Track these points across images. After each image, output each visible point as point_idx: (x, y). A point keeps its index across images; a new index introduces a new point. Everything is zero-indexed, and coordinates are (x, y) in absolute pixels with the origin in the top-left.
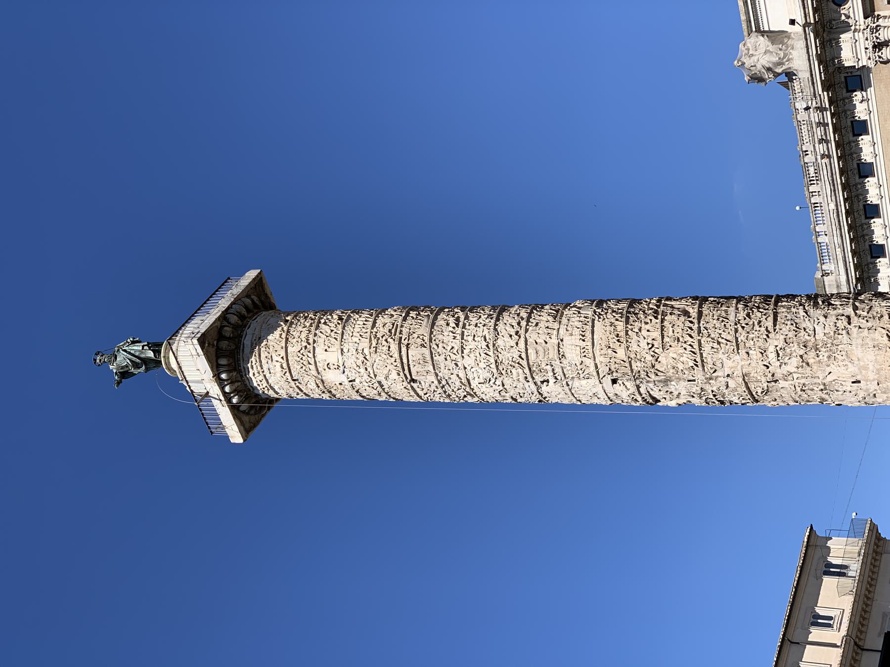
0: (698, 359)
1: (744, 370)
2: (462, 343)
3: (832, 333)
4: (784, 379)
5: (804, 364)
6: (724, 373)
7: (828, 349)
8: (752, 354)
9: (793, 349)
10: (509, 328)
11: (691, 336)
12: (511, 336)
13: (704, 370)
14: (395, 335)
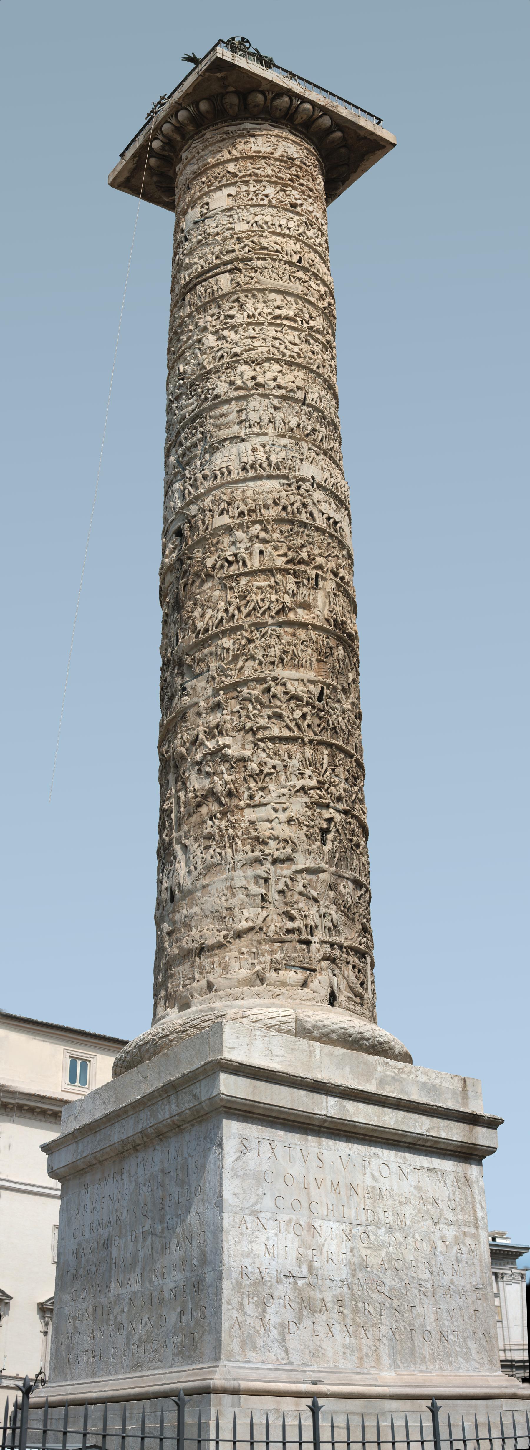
2: (242, 325)
3: (254, 834)
5: (198, 799)
7: (224, 832)
9: (226, 776)
10: (270, 375)
11: (248, 615)
12: (254, 378)
14: (255, 254)
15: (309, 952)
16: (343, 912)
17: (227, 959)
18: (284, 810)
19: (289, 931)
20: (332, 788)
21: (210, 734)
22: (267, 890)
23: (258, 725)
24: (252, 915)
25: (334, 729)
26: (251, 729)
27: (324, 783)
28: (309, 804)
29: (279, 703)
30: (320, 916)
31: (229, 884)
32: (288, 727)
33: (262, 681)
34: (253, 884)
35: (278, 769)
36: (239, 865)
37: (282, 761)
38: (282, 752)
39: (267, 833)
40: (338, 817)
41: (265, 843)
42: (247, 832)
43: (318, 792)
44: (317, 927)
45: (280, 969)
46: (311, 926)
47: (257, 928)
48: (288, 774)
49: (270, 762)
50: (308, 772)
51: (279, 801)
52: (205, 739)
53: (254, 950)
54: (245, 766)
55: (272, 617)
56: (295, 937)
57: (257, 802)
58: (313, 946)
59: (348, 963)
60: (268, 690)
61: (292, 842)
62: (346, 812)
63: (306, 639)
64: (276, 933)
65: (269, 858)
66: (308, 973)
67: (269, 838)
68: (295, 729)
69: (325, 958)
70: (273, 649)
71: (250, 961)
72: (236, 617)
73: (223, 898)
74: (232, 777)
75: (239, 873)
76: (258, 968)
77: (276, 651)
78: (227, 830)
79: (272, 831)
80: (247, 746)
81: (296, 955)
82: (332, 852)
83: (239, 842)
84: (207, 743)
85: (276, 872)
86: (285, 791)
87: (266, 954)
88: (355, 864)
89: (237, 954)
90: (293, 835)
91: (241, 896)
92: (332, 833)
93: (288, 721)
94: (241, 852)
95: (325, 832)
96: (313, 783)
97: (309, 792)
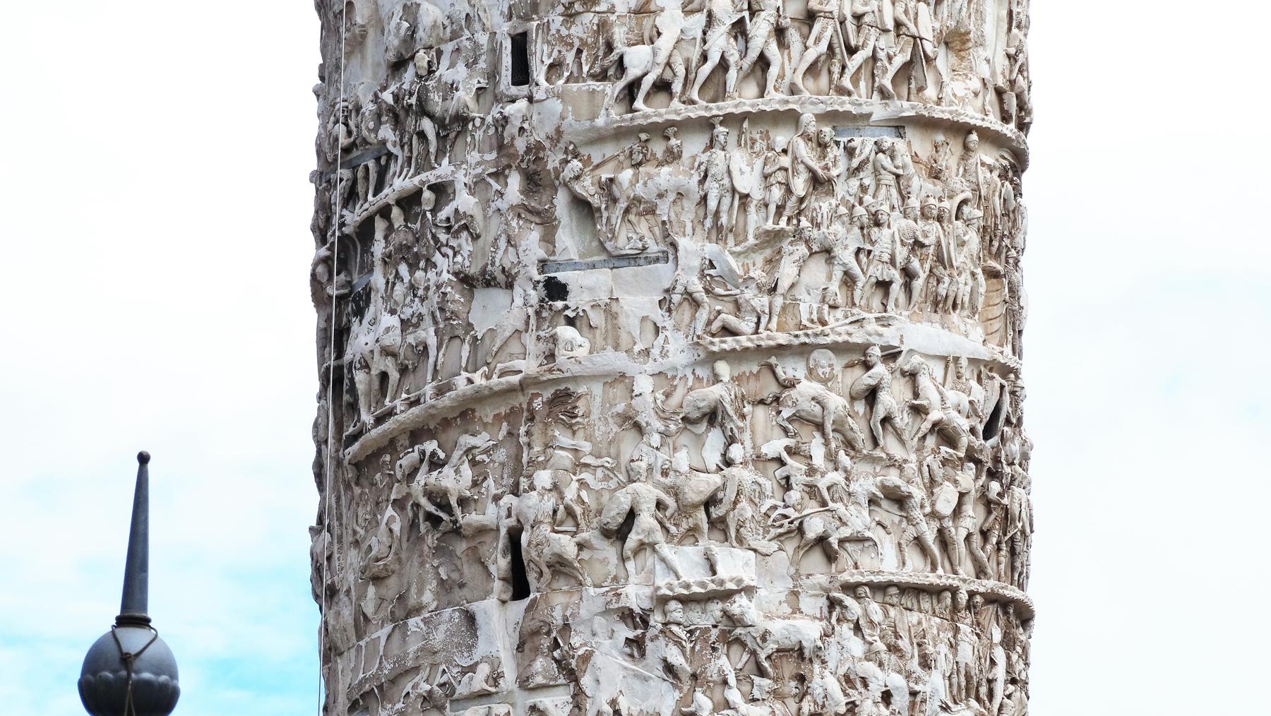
0: (674, 110)
1: (597, 389)
4: (536, 633)
6: (573, 266)
8: (700, 440)
13: (599, 138)
26: (822, 541)
32: (919, 542)
33: (858, 355)
37: (908, 676)
49: (880, 679)
54: (801, 679)
60: (871, 395)
68: (935, 549)
84: (666, 550)
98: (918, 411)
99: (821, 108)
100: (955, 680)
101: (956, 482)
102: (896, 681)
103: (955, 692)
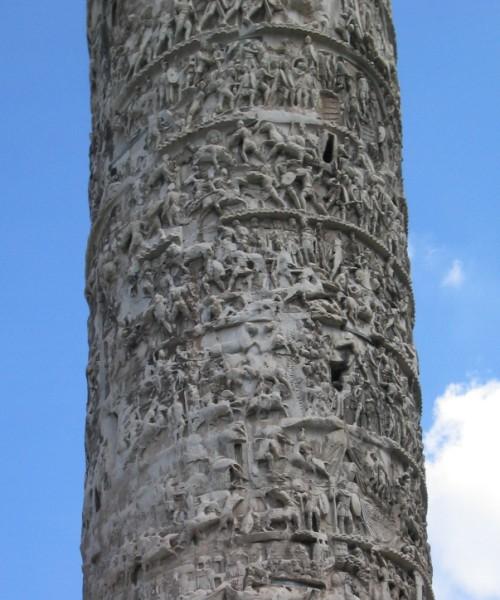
3: (218, 373)
11: (208, 24)
15: (311, 557)
16: (372, 497)
17: (176, 576)
18: (269, 331)
19: (278, 523)
20: (351, 300)
21: (148, 230)
22: (240, 460)
23: (224, 198)
24: (215, 502)
25: (353, 206)
27: (335, 290)
28: (310, 321)
29: (257, 163)
30: (331, 500)
31: (179, 457)
33: (229, 127)
34: (216, 453)
35: (258, 267)
36: (194, 426)
37: (263, 253)
38: (263, 240)
39: (240, 370)
40: (359, 346)
41: (235, 386)
42: (207, 372)
43: (326, 302)
44: (323, 516)
45: (262, 585)
46: (314, 514)
47: (224, 522)
48: (273, 274)
49: (244, 257)
50: (307, 271)
51: (258, 317)
52: (141, 238)
53: (220, 557)
55: (246, 24)
56: (287, 532)
57: (222, 323)
58: (320, 547)
59: (381, 579)
60: (240, 141)
61: (281, 381)
62: (376, 342)
63: (302, 57)
64: (255, 527)
65: (243, 410)
66: (310, 589)
67: (243, 377)
68: (285, 204)
69: (340, 567)
70: (246, 75)
71: (213, 574)
72: (188, 31)
73: (171, 482)
74: (183, 288)
75: (194, 437)
76: (225, 584)
77: (252, 77)
78: (175, 373)
79: (246, 366)
80: (206, 237)
81: (289, 561)
82: (352, 401)
83: (194, 390)
85: (253, 431)
86: (269, 301)
87: (239, 562)
88: (392, 425)
89: (192, 566)
90: (282, 370)
91: (197, 475)
92: (352, 373)
93: (274, 190)
94: (198, 406)
95: (338, 371)
96: (316, 288)
97: (309, 303)
98: (269, 145)
99: (209, 36)
100: (301, 256)
101: (295, 172)
102: (254, 255)
103: (302, 261)
